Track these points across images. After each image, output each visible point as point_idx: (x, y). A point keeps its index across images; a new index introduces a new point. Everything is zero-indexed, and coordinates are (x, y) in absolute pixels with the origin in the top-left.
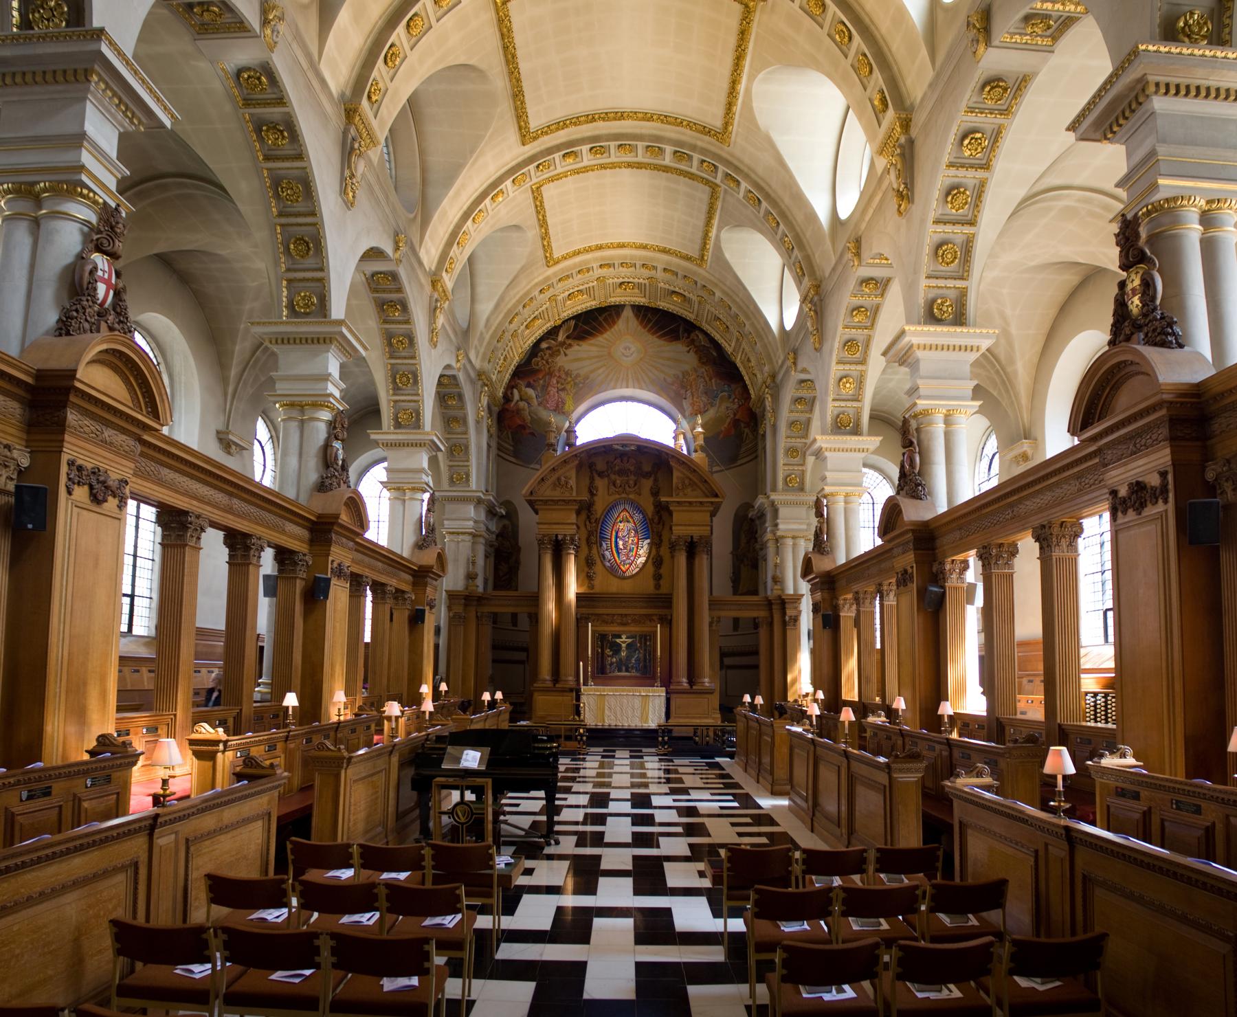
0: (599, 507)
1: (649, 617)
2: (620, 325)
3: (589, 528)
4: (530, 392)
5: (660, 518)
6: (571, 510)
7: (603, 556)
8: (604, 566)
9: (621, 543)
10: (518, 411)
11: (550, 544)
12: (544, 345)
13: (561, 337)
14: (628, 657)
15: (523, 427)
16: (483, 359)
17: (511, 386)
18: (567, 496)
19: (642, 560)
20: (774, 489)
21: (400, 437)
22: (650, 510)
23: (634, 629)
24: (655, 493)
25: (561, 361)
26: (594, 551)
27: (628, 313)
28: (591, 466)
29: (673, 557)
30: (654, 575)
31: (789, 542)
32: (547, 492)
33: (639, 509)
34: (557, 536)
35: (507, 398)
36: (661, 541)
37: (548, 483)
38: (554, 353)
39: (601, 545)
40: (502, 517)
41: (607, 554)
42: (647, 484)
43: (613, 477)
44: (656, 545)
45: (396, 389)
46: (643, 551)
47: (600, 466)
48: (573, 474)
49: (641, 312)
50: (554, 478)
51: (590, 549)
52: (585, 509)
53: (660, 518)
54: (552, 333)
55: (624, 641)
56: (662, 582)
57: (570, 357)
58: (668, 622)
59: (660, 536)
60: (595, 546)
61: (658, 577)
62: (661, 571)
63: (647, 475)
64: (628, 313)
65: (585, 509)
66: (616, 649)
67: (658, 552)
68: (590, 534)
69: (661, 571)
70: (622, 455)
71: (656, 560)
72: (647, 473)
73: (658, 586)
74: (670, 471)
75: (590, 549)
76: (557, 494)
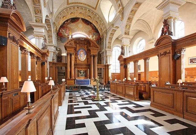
0: (77, 49)
1: (86, 68)
2: (79, 21)
4: (63, 30)
9: (81, 55)
10: (61, 33)
12: (66, 23)
13: (69, 22)
14: (83, 74)
15: (62, 36)
16: (55, 20)
17: (60, 29)
18: (72, 46)
19: (85, 58)
20: (106, 48)
21: (37, 24)
22: (86, 50)
23: (84, 70)
24: (87, 47)
25: (69, 26)
27: (80, 19)
28: (76, 42)
29: (90, 58)
31: (108, 56)
32: (68, 45)
33: (84, 50)
35: (59, 31)
37: (69, 44)
38: (68, 24)
40: (58, 51)
41: (79, 57)
42: (86, 46)
43: (80, 44)
44: (87, 56)
45: (36, 14)
46: (85, 57)
47: (78, 42)
48: (73, 43)
49: (82, 19)
50: (70, 43)
51: (76, 56)
52: (75, 49)
54: (67, 21)
55: (82, 72)
57: (70, 25)
58: (90, 69)
61: (88, 61)
63: (86, 45)
64: (80, 19)
65: (75, 49)
66: (81, 73)
70: (82, 41)
71: (87, 59)
73: (88, 63)
74: (90, 44)
75: (76, 56)
76: (70, 46)
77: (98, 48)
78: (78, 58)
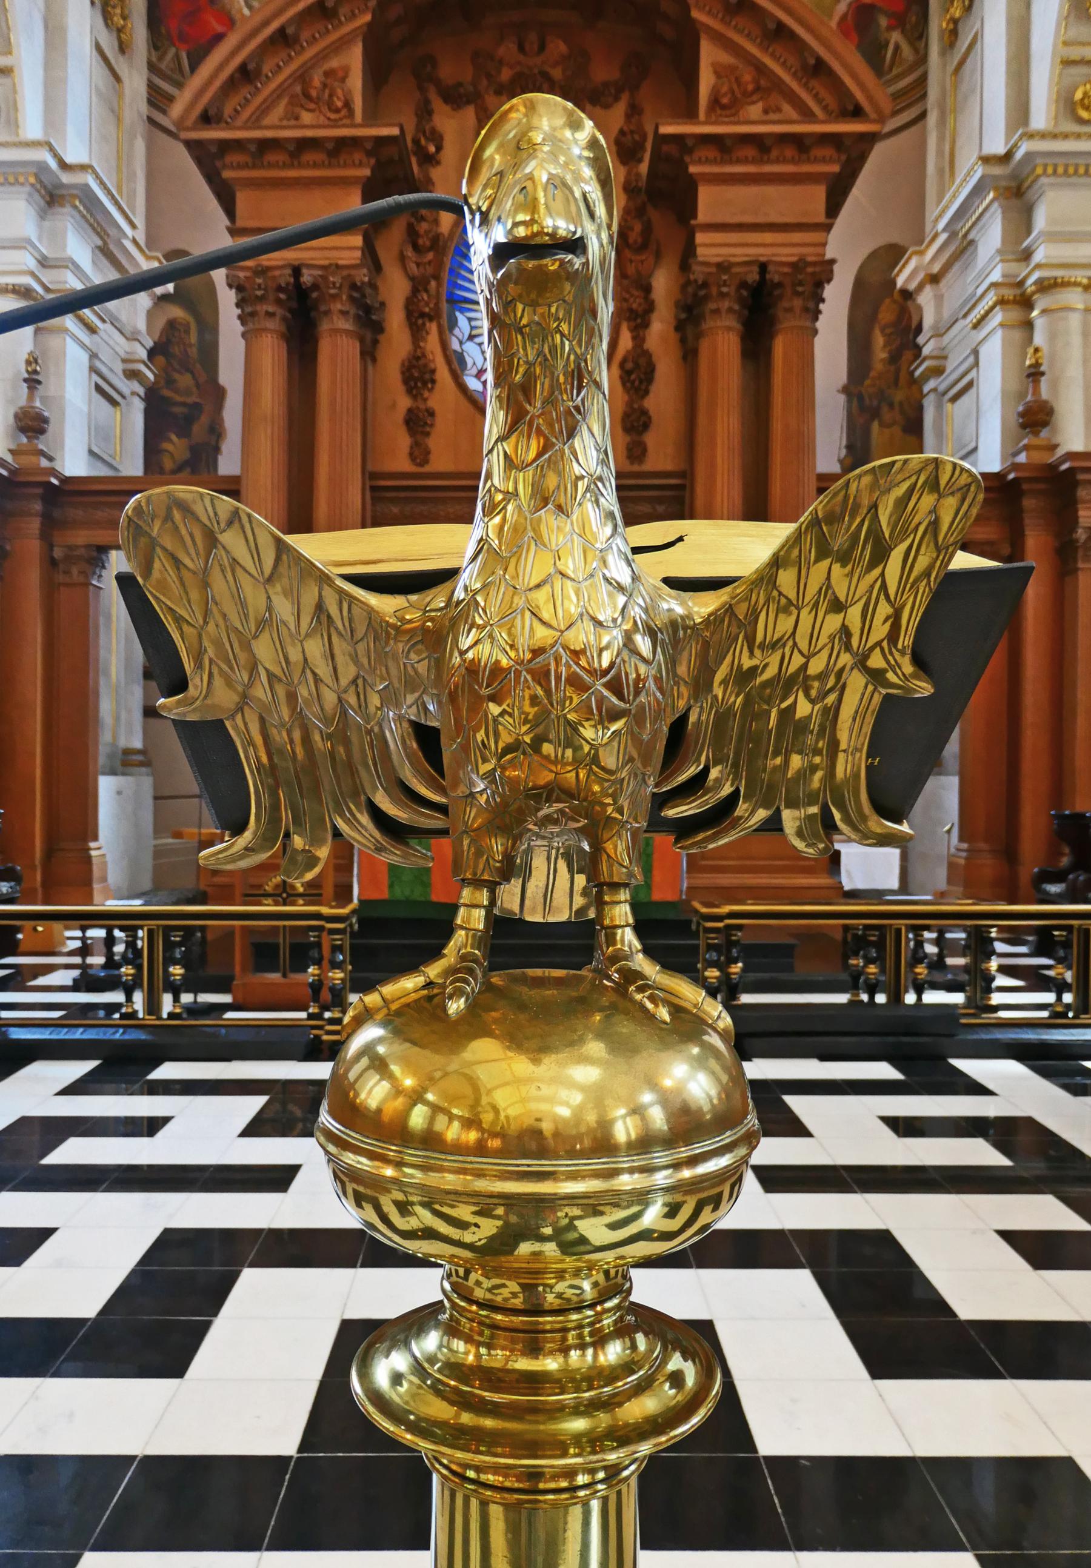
3: (413, 268)
5: (647, 230)
6: (344, 182)
7: (461, 358)
8: (463, 388)
11: (279, 301)
26: (432, 343)
29: (689, 354)
30: (626, 416)
34: (297, 271)
36: (650, 307)
39: (453, 323)
53: (647, 230)
56: (650, 439)
59: (647, 289)
60: (433, 327)
62: (649, 403)
67: (638, 339)
68: (418, 285)
69: (649, 403)
72: (606, 85)
75: (417, 331)
77: (857, 113)
78: (456, 363)
